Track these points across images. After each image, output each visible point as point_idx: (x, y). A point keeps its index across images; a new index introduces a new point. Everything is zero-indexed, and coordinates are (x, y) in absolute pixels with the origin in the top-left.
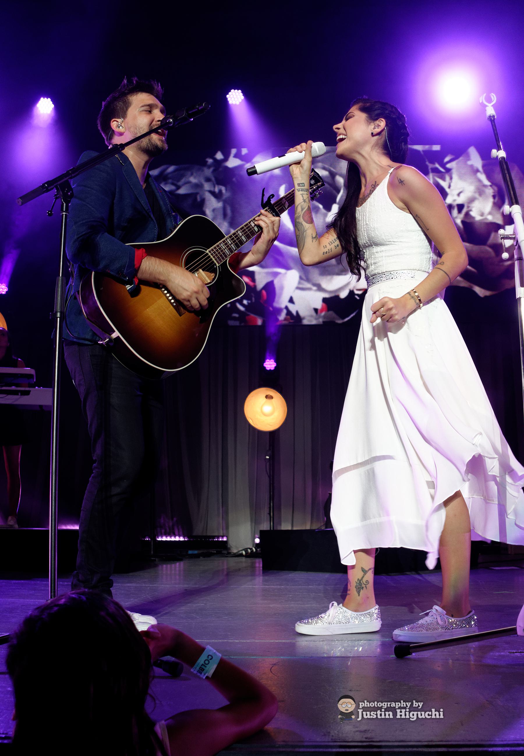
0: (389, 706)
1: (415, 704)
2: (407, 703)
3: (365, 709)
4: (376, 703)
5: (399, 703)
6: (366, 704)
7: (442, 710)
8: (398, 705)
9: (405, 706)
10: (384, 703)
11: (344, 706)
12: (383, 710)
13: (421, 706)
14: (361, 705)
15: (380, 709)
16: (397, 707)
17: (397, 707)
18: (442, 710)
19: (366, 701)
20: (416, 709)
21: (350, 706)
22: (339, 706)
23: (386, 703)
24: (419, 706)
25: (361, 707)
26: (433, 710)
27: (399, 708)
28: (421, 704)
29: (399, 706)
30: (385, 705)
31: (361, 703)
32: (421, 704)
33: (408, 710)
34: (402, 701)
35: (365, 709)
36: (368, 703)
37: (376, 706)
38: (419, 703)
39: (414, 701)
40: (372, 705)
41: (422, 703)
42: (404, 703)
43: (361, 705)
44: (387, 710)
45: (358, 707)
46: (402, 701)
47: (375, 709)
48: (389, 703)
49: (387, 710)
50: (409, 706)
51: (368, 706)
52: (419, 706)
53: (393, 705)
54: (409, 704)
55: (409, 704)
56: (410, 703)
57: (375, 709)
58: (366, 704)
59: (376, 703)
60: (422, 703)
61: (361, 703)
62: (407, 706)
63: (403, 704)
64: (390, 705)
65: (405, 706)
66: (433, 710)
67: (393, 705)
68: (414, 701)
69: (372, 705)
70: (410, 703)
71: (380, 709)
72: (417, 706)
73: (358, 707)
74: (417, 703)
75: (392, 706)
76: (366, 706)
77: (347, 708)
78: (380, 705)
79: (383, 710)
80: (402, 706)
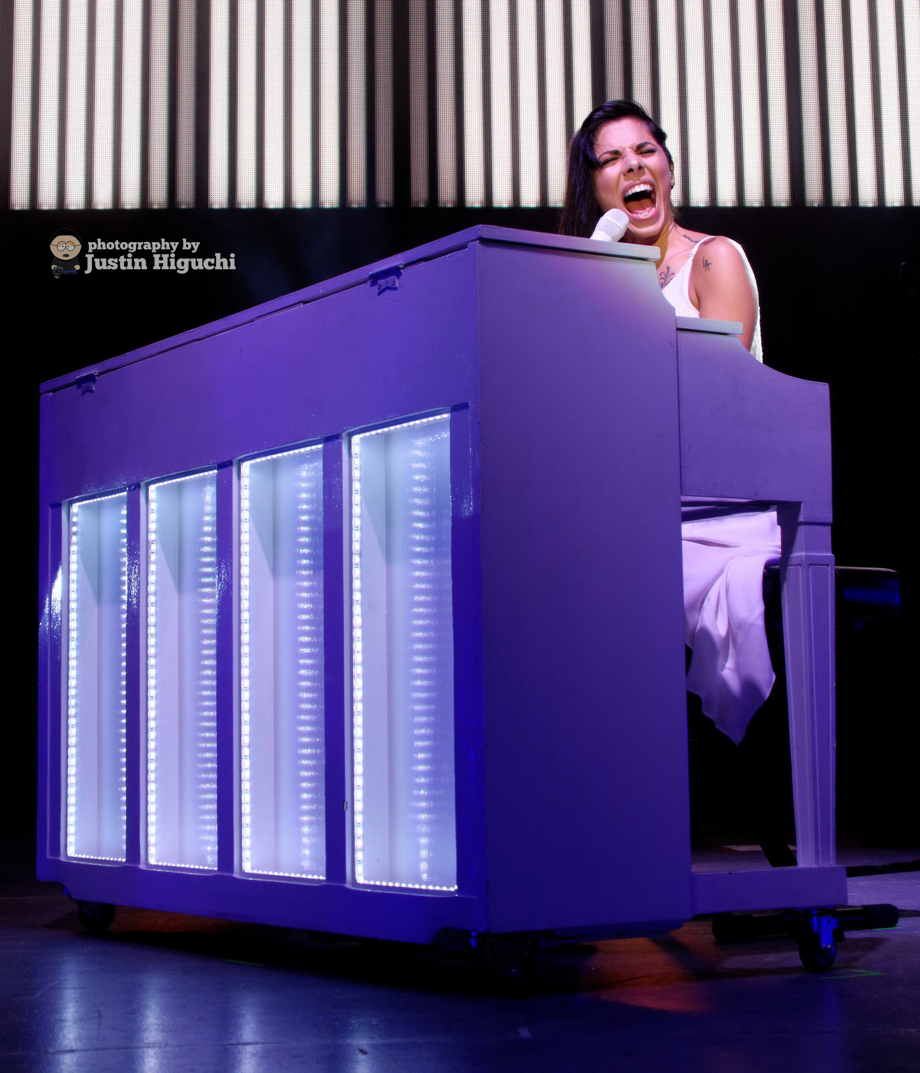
0: (140, 248)
1: (187, 245)
2: (172, 244)
3: (98, 254)
4: (117, 242)
5: (158, 244)
6: (100, 245)
7: (232, 255)
8: (154, 246)
9: (168, 248)
10: (131, 243)
12: (130, 255)
13: (196, 248)
15: (125, 253)
16: (154, 251)
17: (154, 251)
18: (232, 255)
19: (99, 240)
20: (188, 254)
21: (71, 248)
23: (135, 244)
24: (192, 248)
25: (90, 249)
26: (218, 255)
27: (160, 252)
28: (196, 245)
29: (158, 248)
30: (133, 246)
31: (90, 244)
32: (196, 245)
33: (173, 255)
34: (163, 240)
35: (98, 254)
36: (104, 244)
37: (117, 248)
38: (193, 244)
39: (184, 240)
41: (198, 243)
42: (167, 244)
44: (138, 254)
46: (163, 240)
47: (115, 254)
48: (140, 244)
49: (138, 254)
50: (175, 248)
51: (104, 248)
52: (192, 248)
53: (147, 246)
54: (175, 245)
55: (175, 245)
56: (177, 243)
57: (115, 254)
58: (100, 245)
59: (117, 242)
60: (198, 243)
61: (90, 244)
62: (172, 249)
63: (164, 244)
64: (142, 246)
65: (168, 248)
66: (218, 255)
67: (147, 246)
68: (184, 240)
70: (177, 243)
71: (125, 253)
72: (189, 248)
74: (189, 243)
75: (145, 248)
76: (99, 248)
78: (124, 246)
79: (130, 255)
80: (163, 248)
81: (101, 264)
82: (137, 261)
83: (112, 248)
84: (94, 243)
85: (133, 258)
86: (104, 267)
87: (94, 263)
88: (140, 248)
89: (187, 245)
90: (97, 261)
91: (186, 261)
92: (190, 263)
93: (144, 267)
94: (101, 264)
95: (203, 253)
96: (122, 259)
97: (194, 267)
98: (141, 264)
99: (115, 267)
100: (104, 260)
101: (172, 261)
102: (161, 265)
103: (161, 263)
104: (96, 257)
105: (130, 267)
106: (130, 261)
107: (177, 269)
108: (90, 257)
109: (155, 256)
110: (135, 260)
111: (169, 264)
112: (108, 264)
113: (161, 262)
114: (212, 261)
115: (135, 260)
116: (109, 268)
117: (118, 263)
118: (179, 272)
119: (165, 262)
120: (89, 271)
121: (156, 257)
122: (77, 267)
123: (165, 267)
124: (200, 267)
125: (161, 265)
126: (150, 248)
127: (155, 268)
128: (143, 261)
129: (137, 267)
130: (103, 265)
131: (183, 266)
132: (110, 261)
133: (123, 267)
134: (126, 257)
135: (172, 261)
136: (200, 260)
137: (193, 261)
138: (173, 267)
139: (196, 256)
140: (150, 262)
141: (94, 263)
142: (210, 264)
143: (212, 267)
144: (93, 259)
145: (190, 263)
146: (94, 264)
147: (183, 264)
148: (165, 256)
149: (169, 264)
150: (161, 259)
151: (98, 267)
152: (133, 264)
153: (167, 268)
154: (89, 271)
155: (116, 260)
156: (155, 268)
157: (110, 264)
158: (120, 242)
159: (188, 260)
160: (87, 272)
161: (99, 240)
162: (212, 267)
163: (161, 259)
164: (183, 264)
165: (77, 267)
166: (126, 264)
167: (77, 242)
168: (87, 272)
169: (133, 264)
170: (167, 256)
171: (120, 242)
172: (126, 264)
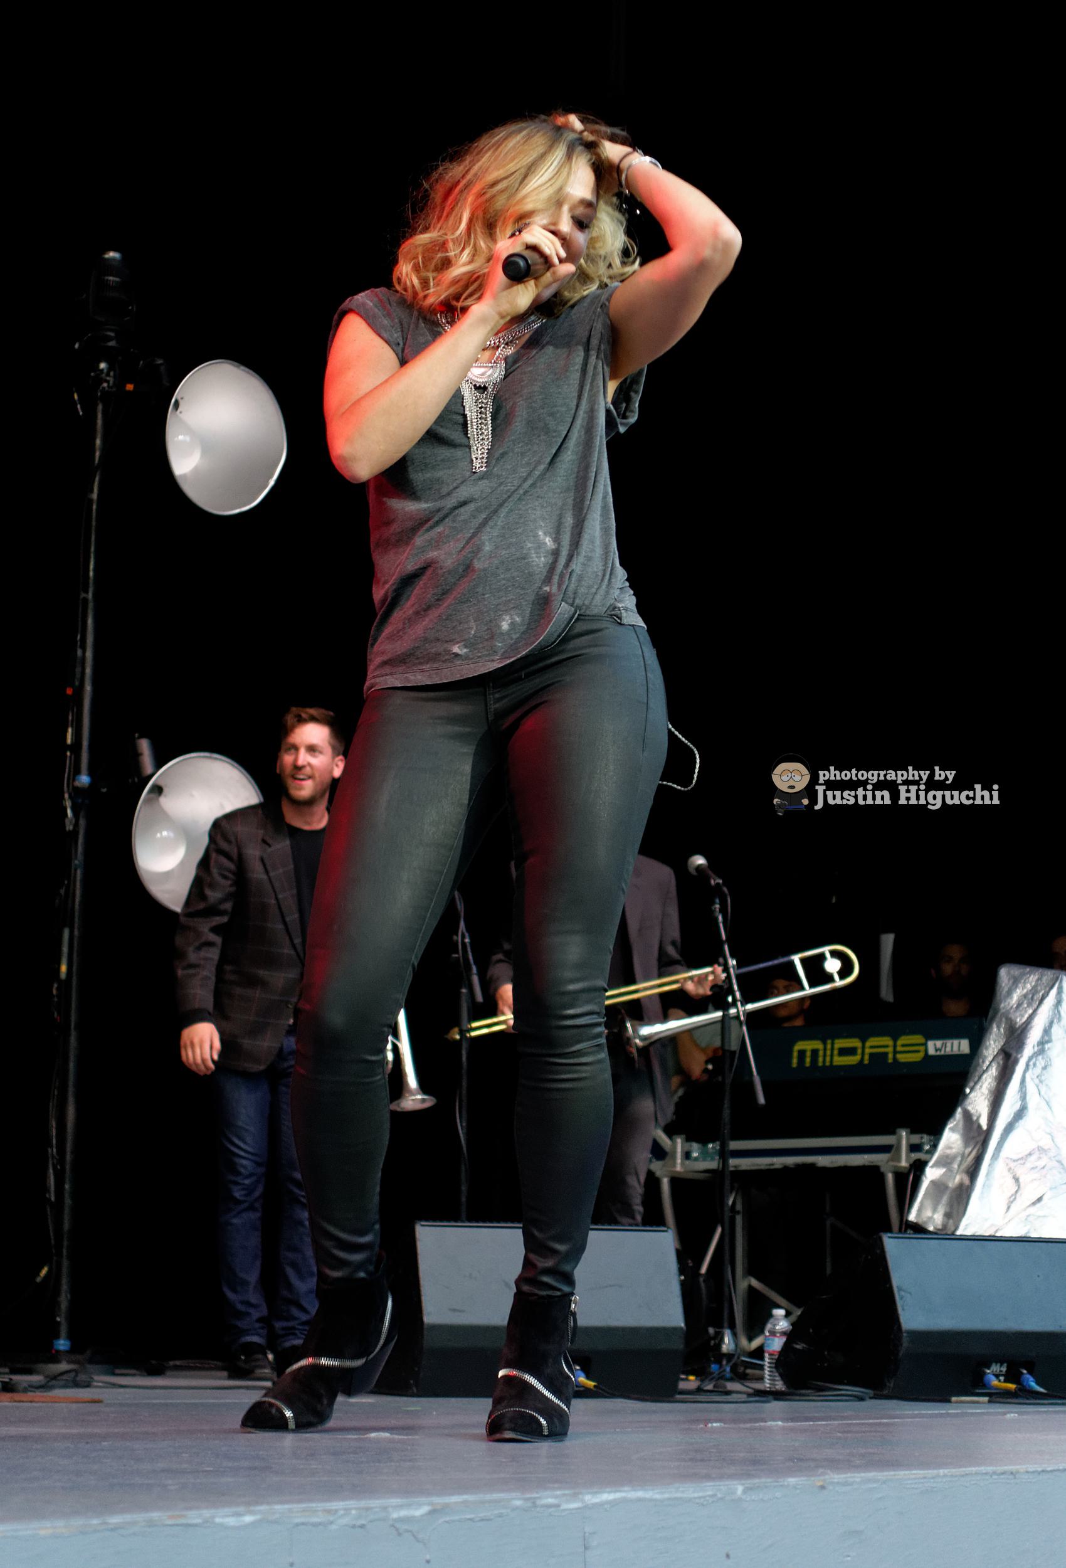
0: (882, 778)
1: (939, 774)
2: (922, 773)
3: (831, 785)
4: (854, 771)
5: (904, 773)
6: (833, 774)
8: (899, 776)
9: (917, 778)
10: (871, 772)
11: (785, 778)
12: (870, 787)
13: (951, 778)
14: (823, 776)
15: (864, 784)
16: (899, 781)
17: (899, 781)
19: (832, 768)
20: (941, 786)
21: (797, 778)
22: (775, 779)
23: (876, 773)
24: (947, 778)
25: (821, 781)
27: (906, 782)
28: (951, 775)
29: (905, 778)
30: (873, 776)
31: (821, 773)
32: (951, 775)
33: (922, 787)
34: (910, 768)
35: (831, 785)
36: (837, 772)
37: (854, 778)
38: (948, 773)
39: (937, 768)
40: (846, 775)
41: (954, 772)
42: (916, 772)
43: (823, 776)
44: (880, 785)
45: (814, 780)
46: (910, 768)
47: (852, 785)
48: (882, 773)
49: (880, 785)
50: (925, 778)
51: (838, 778)
52: (947, 778)
53: (891, 775)
54: (925, 775)
55: (925, 775)
56: (928, 772)
57: (852, 785)
58: (833, 774)
59: (854, 771)
60: (954, 772)
61: (821, 773)
62: (921, 779)
63: (912, 773)
64: (885, 776)
65: (917, 778)
67: (891, 775)
68: (937, 768)
69: (846, 775)
70: (928, 772)
71: (864, 784)
72: (943, 778)
73: (814, 780)
74: (942, 772)
75: (888, 778)
76: (832, 778)
77: (792, 783)
78: (863, 775)
79: (870, 787)
80: (911, 778)
81: (834, 798)
82: (878, 794)
83: (848, 778)
84: (826, 772)
85: (873, 790)
86: (838, 801)
87: (825, 797)
88: (882, 778)
89: (939, 774)
90: (829, 793)
91: (939, 794)
92: (943, 796)
93: (888, 801)
94: (834, 798)
95: (959, 785)
96: (860, 792)
97: (949, 801)
98: (883, 798)
99: (852, 801)
100: (838, 793)
101: (922, 794)
102: (908, 799)
103: (908, 796)
104: (828, 789)
105: (870, 801)
106: (869, 794)
107: (928, 803)
108: (820, 789)
109: (900, 787)
110: (876, 792)
111: (918, 798)
112: (842, 798)
113: (908, 795)
114: (971, 794)
115: (876, 792)
116: (845, 802)
117: (856, 797)
118: (930, 807)
119: (913, 795)
120: (819, 806)
121: (902, 789)
122: (806, 802)
123: (913, 801)
124: (956, 801)
125: (908, 799)
126: (894, 778)
127: (900, 802)
128: (886, 794)
129: (878, 802)
130: (837, 798)
131: (935, 801)
132: (846, 793)
133: (861, 802)
134: (865, 789)
135: (922, 794)
136: (956, 793)
137: (948, 793)
138: (922, 802)
139: (951, 788)
140: (895, 796)
141: (825, 797)
142: (968, 798)
143: (971, 802)
144: (825, 791)
145: (943, 796)
146: (825, 797)
147: (935, 797)
148: (913, 788)
149: (918, 798)
150: (908, 791)
151: (831, 801)
152: (874, 798)
153: (916, 802)
154: (819, 806)
155: (853, 793)
156: (900, 802)
157: (847, 798)
158: (858, 770)
159: (941, 792)
160: (816, 808)
161: (832, 768)
162: (971, 802)
163: (908, 791)
164: (935, 797)
165: (806, 802)
166: (865, 798)
167: (804, 770)
168: (816, 808)
169: (874, 798)
170: (916, 787)
171: (858, 770)
172: (865, 798)
